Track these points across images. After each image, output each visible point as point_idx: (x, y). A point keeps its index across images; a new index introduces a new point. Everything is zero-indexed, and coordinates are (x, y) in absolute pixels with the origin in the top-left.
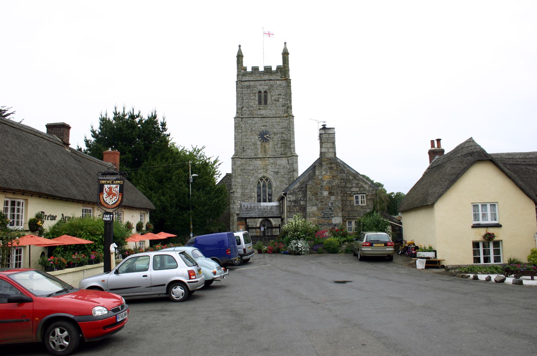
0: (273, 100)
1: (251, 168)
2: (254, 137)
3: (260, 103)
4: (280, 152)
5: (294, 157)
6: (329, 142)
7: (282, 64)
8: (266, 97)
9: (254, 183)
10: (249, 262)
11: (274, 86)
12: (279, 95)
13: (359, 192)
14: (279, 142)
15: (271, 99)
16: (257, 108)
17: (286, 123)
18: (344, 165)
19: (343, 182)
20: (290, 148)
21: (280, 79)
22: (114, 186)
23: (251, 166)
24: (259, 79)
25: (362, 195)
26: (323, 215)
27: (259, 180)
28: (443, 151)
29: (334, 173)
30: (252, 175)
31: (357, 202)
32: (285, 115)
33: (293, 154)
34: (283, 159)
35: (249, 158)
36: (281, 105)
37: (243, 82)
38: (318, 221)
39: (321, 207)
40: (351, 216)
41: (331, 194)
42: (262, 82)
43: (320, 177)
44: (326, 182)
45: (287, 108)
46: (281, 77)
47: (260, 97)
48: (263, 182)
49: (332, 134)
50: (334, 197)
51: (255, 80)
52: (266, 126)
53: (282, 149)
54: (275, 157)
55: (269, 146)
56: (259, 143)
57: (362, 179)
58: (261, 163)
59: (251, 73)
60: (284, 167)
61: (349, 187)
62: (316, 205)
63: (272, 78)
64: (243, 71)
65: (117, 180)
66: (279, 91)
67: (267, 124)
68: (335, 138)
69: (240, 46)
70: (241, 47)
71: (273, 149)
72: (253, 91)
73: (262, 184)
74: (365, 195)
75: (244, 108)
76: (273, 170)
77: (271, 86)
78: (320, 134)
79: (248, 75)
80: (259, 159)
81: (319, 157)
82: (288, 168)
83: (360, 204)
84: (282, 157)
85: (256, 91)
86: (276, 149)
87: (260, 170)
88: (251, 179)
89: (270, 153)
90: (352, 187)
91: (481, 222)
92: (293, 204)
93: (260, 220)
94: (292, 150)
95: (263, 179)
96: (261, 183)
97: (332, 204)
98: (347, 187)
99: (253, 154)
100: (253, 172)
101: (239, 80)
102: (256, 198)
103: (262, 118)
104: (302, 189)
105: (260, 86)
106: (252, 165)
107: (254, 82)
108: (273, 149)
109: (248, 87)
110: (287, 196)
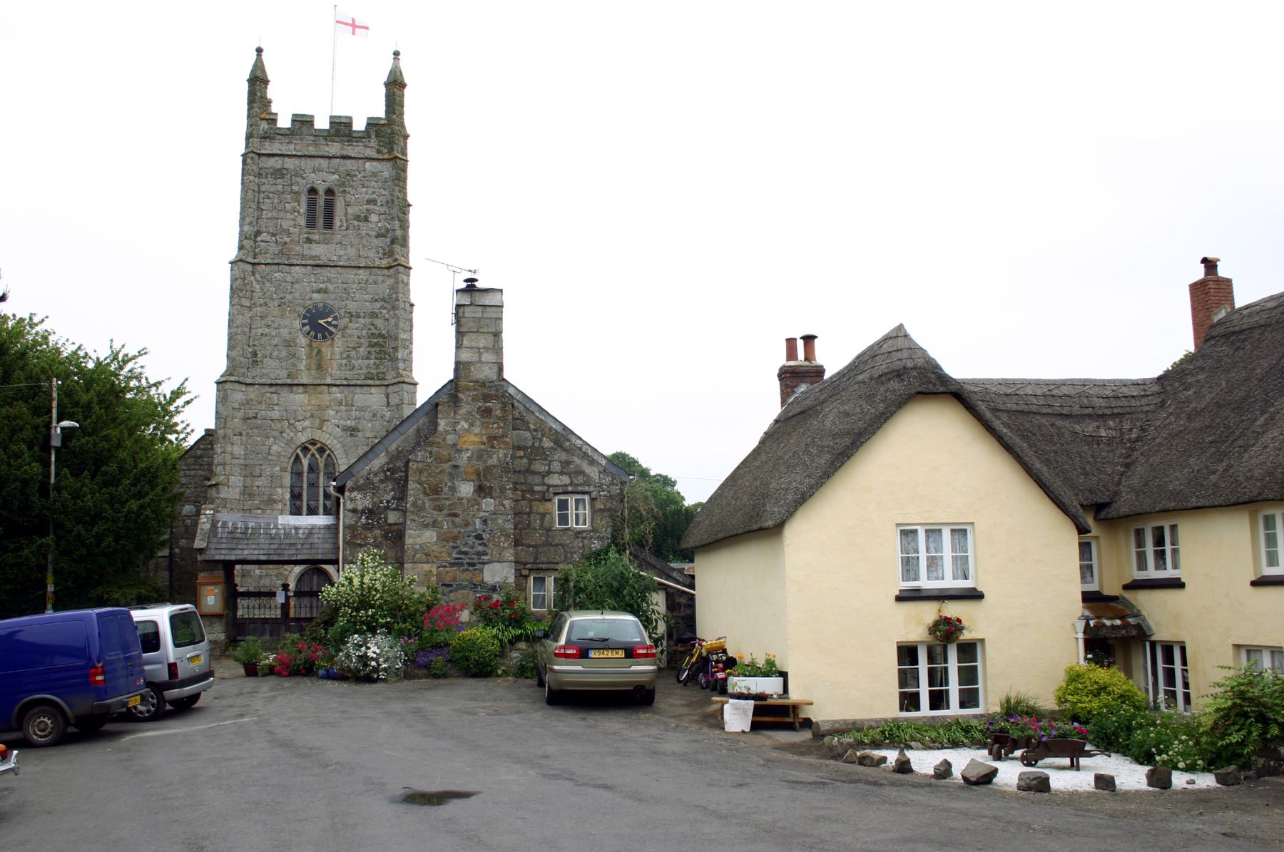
0: (352, 218)
1: (276, 414)
2: (287, 322)
3: (311, 223)
4: (364, 371)
5: (404, 385)
6: (482, 330)
7: (383, 115)
8: (330, 206)
9: (282, 459)
10: (196, 705)
11: (355, 176)
12: (369, 202)
13: (570, 489)
14: (362, 341)
15: (346, 213)
16: (301, 236)
17: (386, 285)
18: (528, 405)
19: (521, 458)
20: (394, 360)
21: (376, 156)
23: (276, 407)
24: (312, 150)
25: (579, 497)
26: (455, 556)
27: (299, 451)
28: (820, 371)
29: (496, 429)
31: (564, 519)
32: (385, 262)
33: (402, 376)
34: (373, 390)
36: (374, 233)
37: (263, 158)
38: (439, 575)
39: (451, 532)
40: (544, 559)
41: (482, 490)
42: (322, 161)
43: (451, 439)
44: (468, 455)
45: (393, 242)
46: (379, 152)
47: (312, 206)
48: (309, 456)
49: (494, 309)
50: (492, 501)
51: (299, 154)
52: (325, 291)
53: (372, 361)
55: (334, 350)
56: (303, 341)
57: (580, 449)
58: (306, 402)
59: (288, 133)
60: (374, 415)
61: (540, 473)
62: (435, 524)
63: (350, 151)
64: (264, 125)
66: (370, 190)
67: (331, 287)
68: (501, 319)
69: (259, 51)
70: (263, 54)
71: (344, 362)
72: (293, 187)
73: (305, 462)
74: (586, 498)
75: (264, 236)
76: (342, 422)
77: (349, 175)
78: (458, 306)
79: (279, 137)
80: (301, 388)
81: (451, 377)
82: (387, 418)
83: (572, 524)
84: (368, 386)
85: (301, 186)
86: (353, 361)
87: (303, 420)
88: (275, 448)
89: (334, 372)
90: (549, 473)
91: (925, 583)
92: (363, 520)
93: (298, 569)
94: (401, 365)
95: (310, 447)
96: (303, 460)
97: (485, 522)
98: (534, 473)
99: (284, 374)
100: (282, 427)
101: (252, 152)
102: (285, 505)
103: (315, 268)
104: (392, 473)
105: (314, 172)
107: (296, 161)
108: (344, 362)
109: (279, 173)
110: (347, 493)
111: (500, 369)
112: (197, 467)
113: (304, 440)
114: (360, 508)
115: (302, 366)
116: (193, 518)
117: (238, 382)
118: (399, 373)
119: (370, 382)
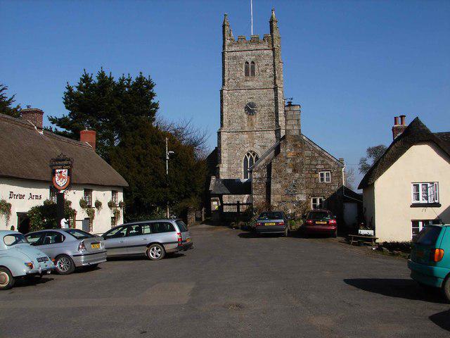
1: (237, 142)
3: (247, 74)
8: (253, 68)
12: (266, 65)
22: (64, 170)
24: (245, 49)
29: (298, 151)
31: (322, 179)
38: (282, 198)
41: (295, 171)
55: (256, 119)
56: (245, 116)
63: (259, 47)
65: (66, 165)
83: (325, 181)
89: (257, 126)
91: (422, 201)
109: (235, 58)
111: (300, 130)
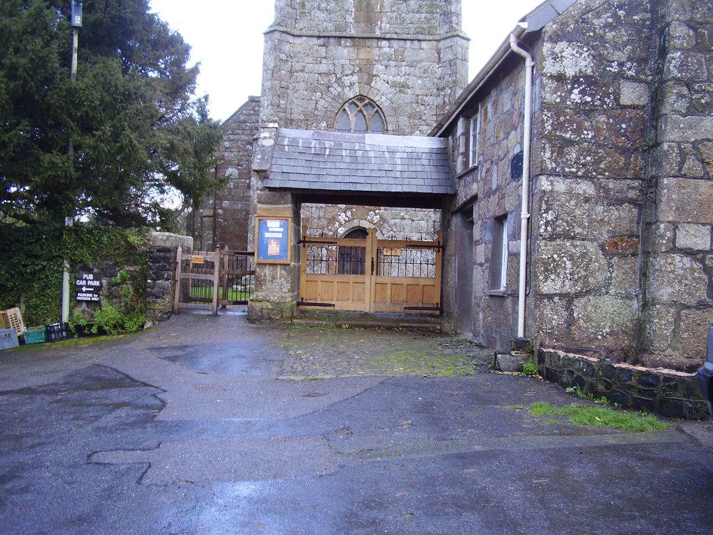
5: (458, 39)
23: (324, 61)
30: (324, 88)
35: (319, 37)
53: (423, 16)
54: (398, 39)
58: (355, 56)
80: (349, 40)
82: (438, 76)
87: (352, 74)
88: (322, 102)
89: (384, 26)
92: (575, 96)
94: (454, 19)
95: (358, 103)
99: (330, 26)
100: (329, 81)
104: (628, 14)
106: (325, 58)
108: (394, 15)
112: (240, 132)
113: (352, 96)
114: (570, 72)
115: (350, 19)
116: (236, 181)
117: (286, 33)
118: (452, 27)
119: (421, 37)
